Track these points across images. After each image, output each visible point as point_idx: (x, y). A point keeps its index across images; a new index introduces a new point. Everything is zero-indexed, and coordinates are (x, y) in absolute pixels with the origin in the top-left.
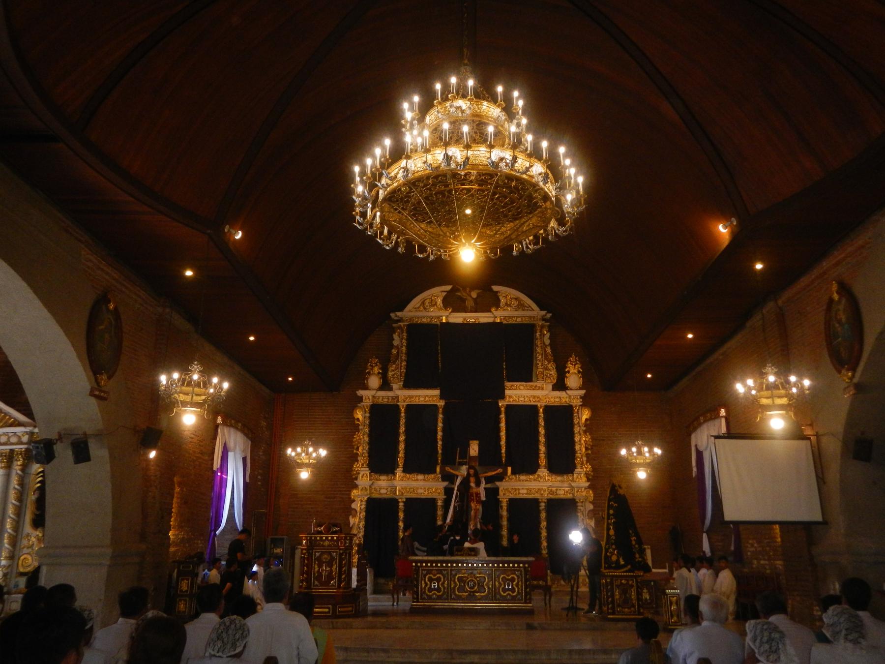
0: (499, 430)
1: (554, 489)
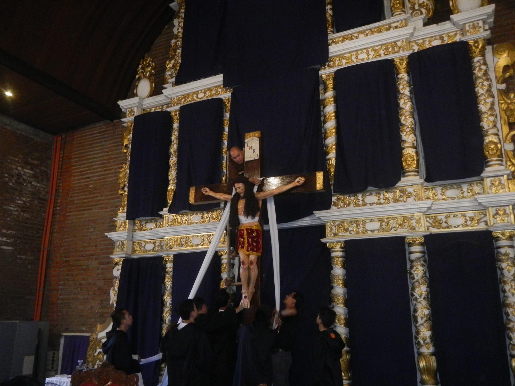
1: (442, 217)
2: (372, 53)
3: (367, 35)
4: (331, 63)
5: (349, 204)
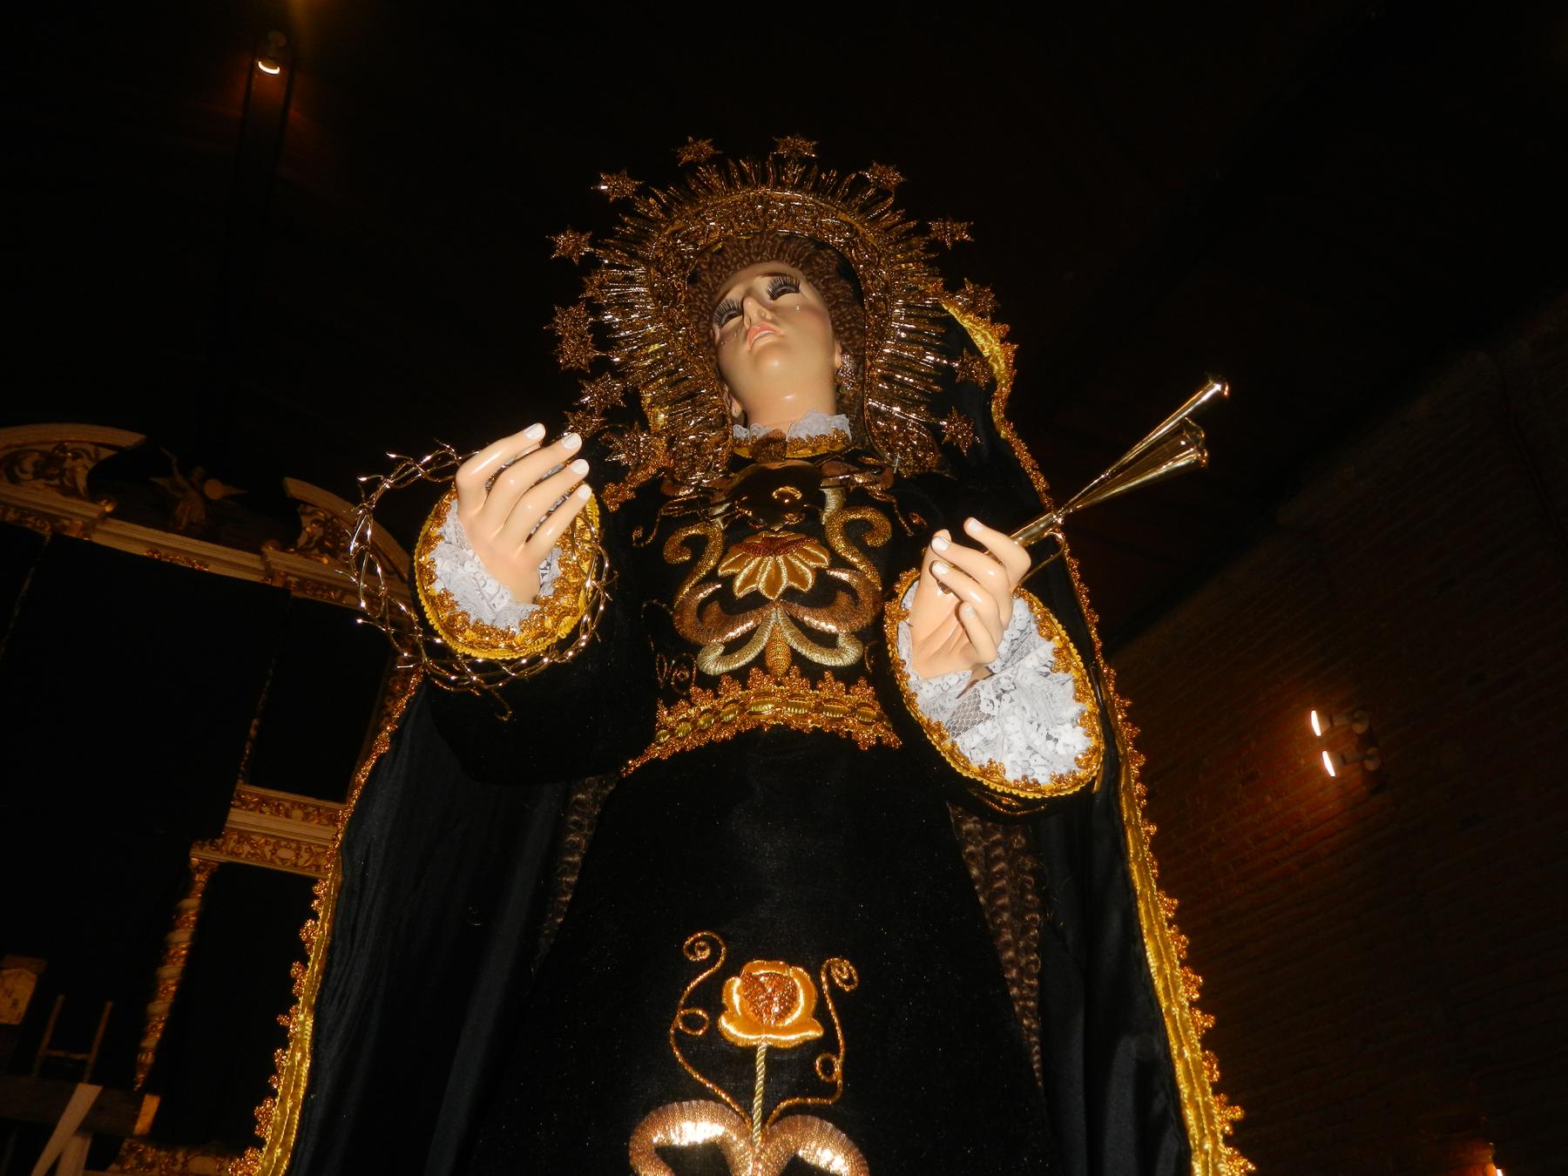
0: (158, 953)
2: (305, 856)
3: (306, 817)
4: (220, 841)
5: (151, 1166)
